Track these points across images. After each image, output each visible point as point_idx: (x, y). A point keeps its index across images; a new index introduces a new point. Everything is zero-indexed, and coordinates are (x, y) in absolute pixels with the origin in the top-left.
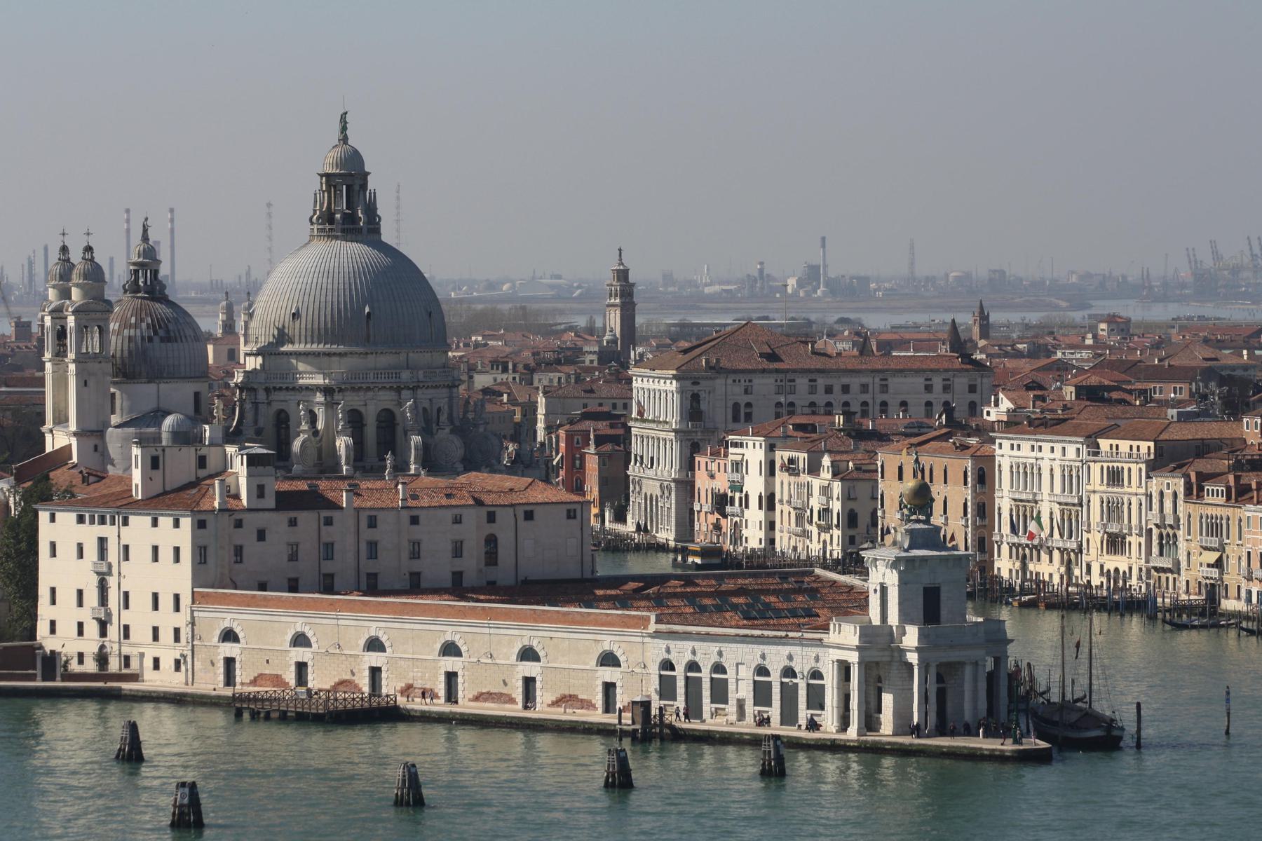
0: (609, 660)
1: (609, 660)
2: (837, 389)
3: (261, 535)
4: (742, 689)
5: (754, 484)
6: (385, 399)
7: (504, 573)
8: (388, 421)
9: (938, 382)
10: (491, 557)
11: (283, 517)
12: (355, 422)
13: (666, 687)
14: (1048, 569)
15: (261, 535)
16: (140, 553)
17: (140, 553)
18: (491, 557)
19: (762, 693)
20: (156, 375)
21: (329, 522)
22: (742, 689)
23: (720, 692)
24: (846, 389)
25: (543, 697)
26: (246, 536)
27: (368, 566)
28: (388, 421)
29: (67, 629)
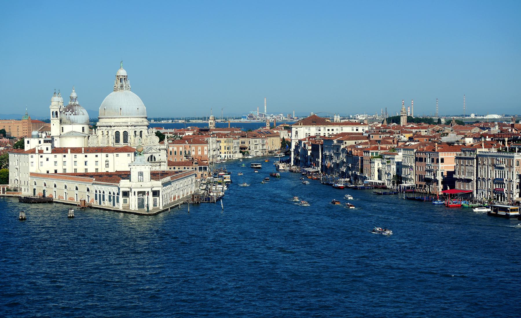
2: (331, 130)
3: (47, 160)
6: (125, 129)
8: (126, 134)
9: (355, 129)
10: (107, 165)
11: (53, 155)
12: (117, 133)
15: (47, 160)
18: (107, 165)
20: (72, 123)
21: (65, 156)
24: (333, 130)
27: (86, 167)
28: (126, 134)
29: (13, 182)
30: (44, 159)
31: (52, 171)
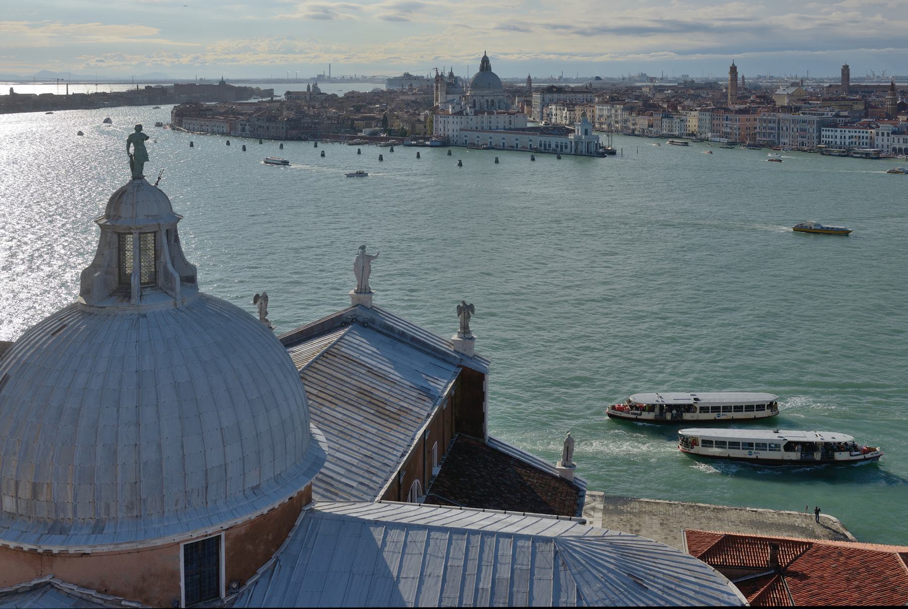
0: (531, 140)
1: (531, 140)
4: (553, 146)
5: (554, 112)
6: (492, 98)
7: (512, 127)
8: (493, 101)
12: (487, 101)
13: (541, 145)
14: (605, 127)
16: (451, 122)
17: (451, 122)
19: (557, 146)
22: (553, 146)
23: (550, 146)
25: (519, 146)
26: (469, 120)
28: (493, 101)
30: (469, 120)
31: (474, 128)
